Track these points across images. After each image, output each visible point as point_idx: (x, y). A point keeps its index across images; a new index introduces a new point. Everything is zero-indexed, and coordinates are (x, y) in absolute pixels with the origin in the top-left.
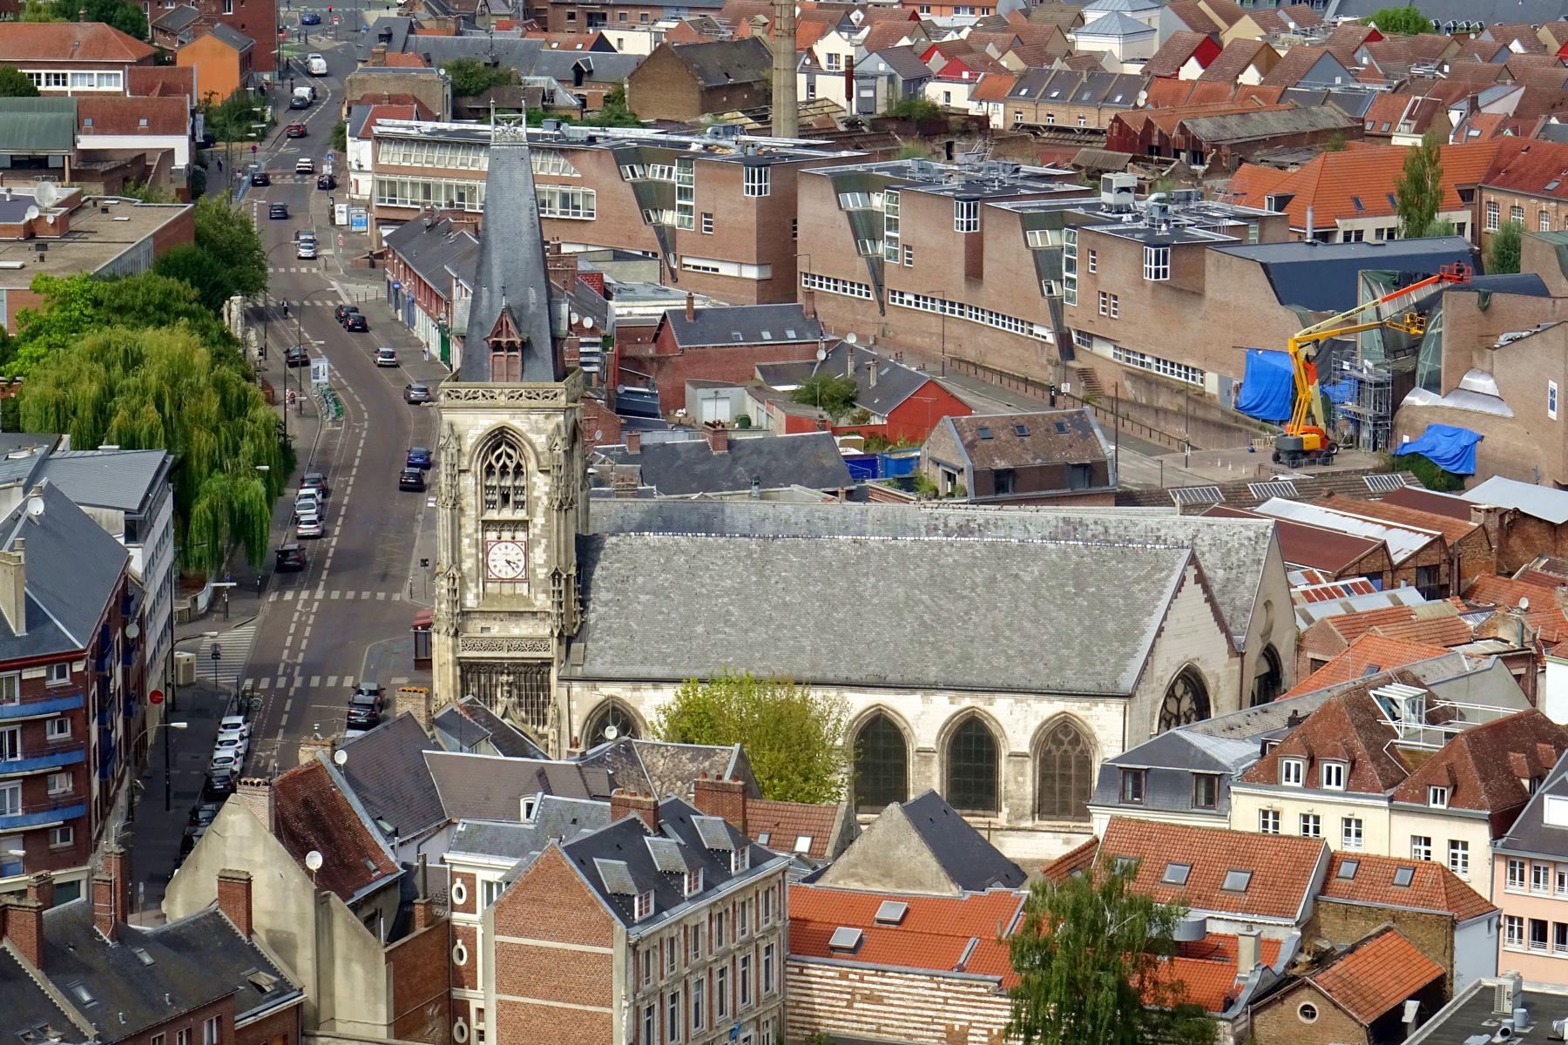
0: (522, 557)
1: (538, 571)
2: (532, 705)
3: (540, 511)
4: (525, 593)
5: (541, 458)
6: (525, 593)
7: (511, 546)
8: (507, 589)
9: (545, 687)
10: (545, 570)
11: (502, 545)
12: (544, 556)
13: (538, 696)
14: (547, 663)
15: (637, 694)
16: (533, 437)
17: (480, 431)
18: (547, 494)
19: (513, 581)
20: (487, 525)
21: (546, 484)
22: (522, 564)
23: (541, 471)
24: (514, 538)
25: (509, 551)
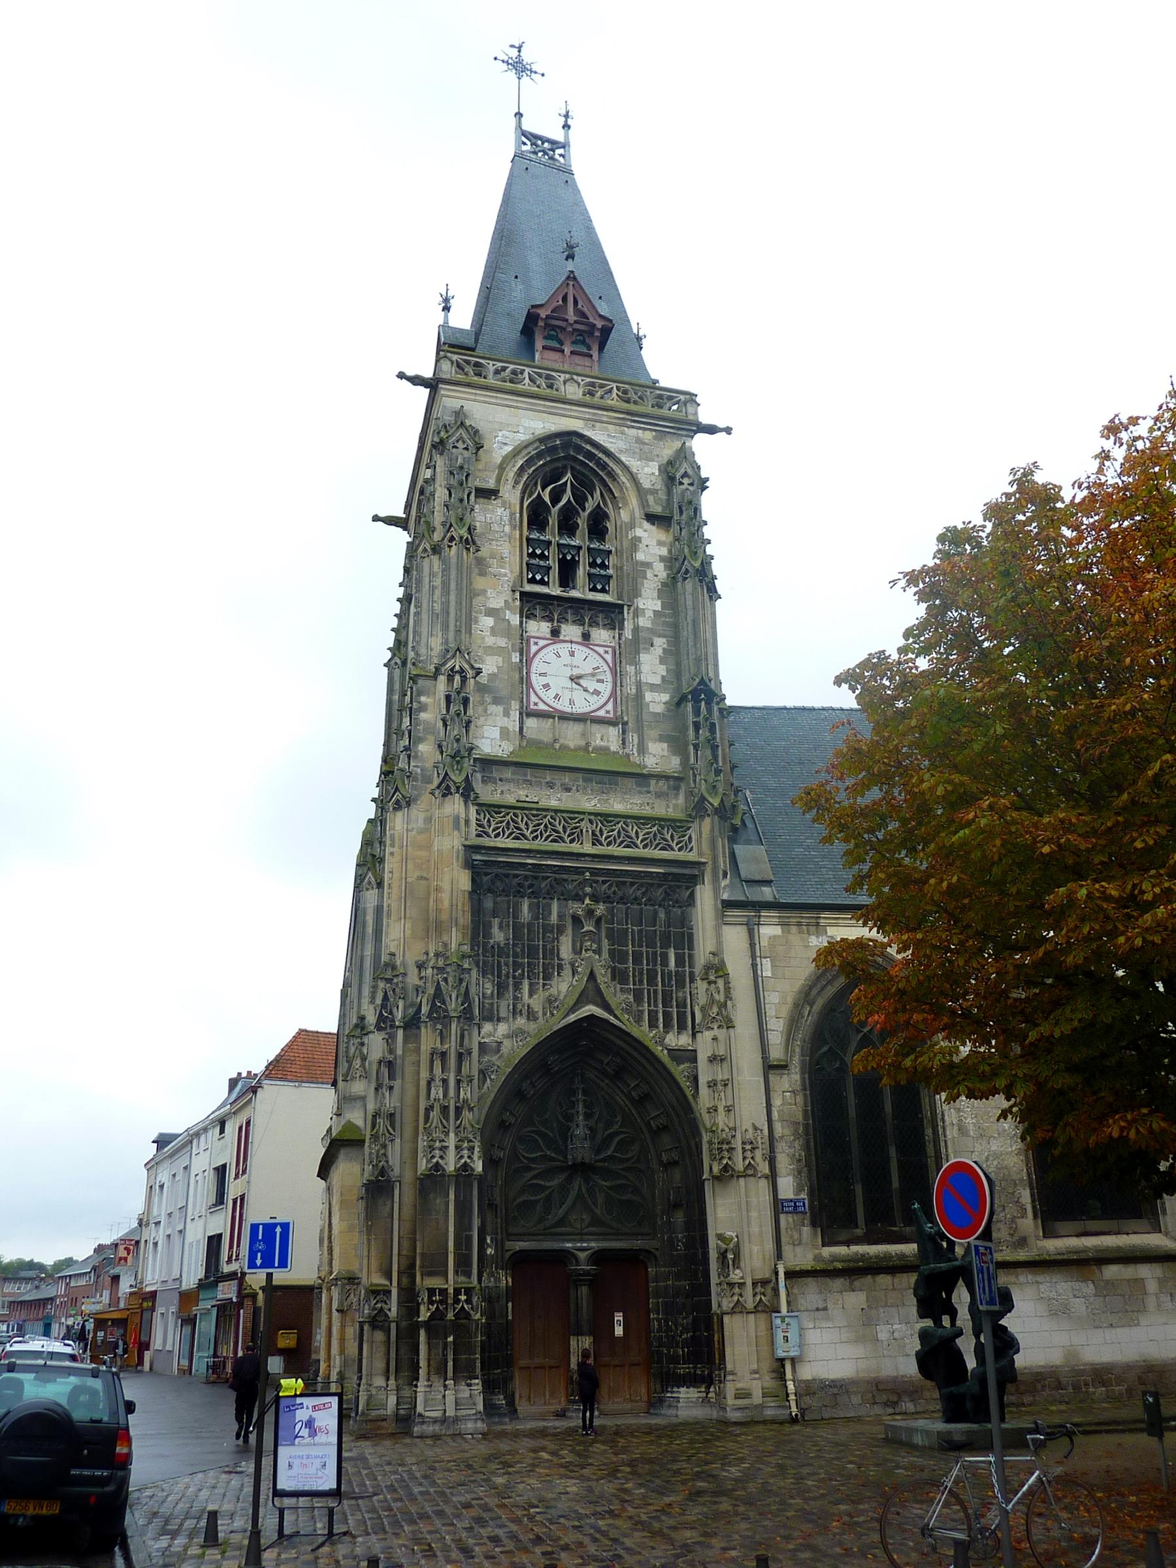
1: (649, 696)
2: (652, 980)
4: (614, 746)
6: (614, 746)
7: (581, 651)
8: (571, 735)
11: (563, 649)
13: (665, 957)
20: (532, 604)
24: (586, 636)
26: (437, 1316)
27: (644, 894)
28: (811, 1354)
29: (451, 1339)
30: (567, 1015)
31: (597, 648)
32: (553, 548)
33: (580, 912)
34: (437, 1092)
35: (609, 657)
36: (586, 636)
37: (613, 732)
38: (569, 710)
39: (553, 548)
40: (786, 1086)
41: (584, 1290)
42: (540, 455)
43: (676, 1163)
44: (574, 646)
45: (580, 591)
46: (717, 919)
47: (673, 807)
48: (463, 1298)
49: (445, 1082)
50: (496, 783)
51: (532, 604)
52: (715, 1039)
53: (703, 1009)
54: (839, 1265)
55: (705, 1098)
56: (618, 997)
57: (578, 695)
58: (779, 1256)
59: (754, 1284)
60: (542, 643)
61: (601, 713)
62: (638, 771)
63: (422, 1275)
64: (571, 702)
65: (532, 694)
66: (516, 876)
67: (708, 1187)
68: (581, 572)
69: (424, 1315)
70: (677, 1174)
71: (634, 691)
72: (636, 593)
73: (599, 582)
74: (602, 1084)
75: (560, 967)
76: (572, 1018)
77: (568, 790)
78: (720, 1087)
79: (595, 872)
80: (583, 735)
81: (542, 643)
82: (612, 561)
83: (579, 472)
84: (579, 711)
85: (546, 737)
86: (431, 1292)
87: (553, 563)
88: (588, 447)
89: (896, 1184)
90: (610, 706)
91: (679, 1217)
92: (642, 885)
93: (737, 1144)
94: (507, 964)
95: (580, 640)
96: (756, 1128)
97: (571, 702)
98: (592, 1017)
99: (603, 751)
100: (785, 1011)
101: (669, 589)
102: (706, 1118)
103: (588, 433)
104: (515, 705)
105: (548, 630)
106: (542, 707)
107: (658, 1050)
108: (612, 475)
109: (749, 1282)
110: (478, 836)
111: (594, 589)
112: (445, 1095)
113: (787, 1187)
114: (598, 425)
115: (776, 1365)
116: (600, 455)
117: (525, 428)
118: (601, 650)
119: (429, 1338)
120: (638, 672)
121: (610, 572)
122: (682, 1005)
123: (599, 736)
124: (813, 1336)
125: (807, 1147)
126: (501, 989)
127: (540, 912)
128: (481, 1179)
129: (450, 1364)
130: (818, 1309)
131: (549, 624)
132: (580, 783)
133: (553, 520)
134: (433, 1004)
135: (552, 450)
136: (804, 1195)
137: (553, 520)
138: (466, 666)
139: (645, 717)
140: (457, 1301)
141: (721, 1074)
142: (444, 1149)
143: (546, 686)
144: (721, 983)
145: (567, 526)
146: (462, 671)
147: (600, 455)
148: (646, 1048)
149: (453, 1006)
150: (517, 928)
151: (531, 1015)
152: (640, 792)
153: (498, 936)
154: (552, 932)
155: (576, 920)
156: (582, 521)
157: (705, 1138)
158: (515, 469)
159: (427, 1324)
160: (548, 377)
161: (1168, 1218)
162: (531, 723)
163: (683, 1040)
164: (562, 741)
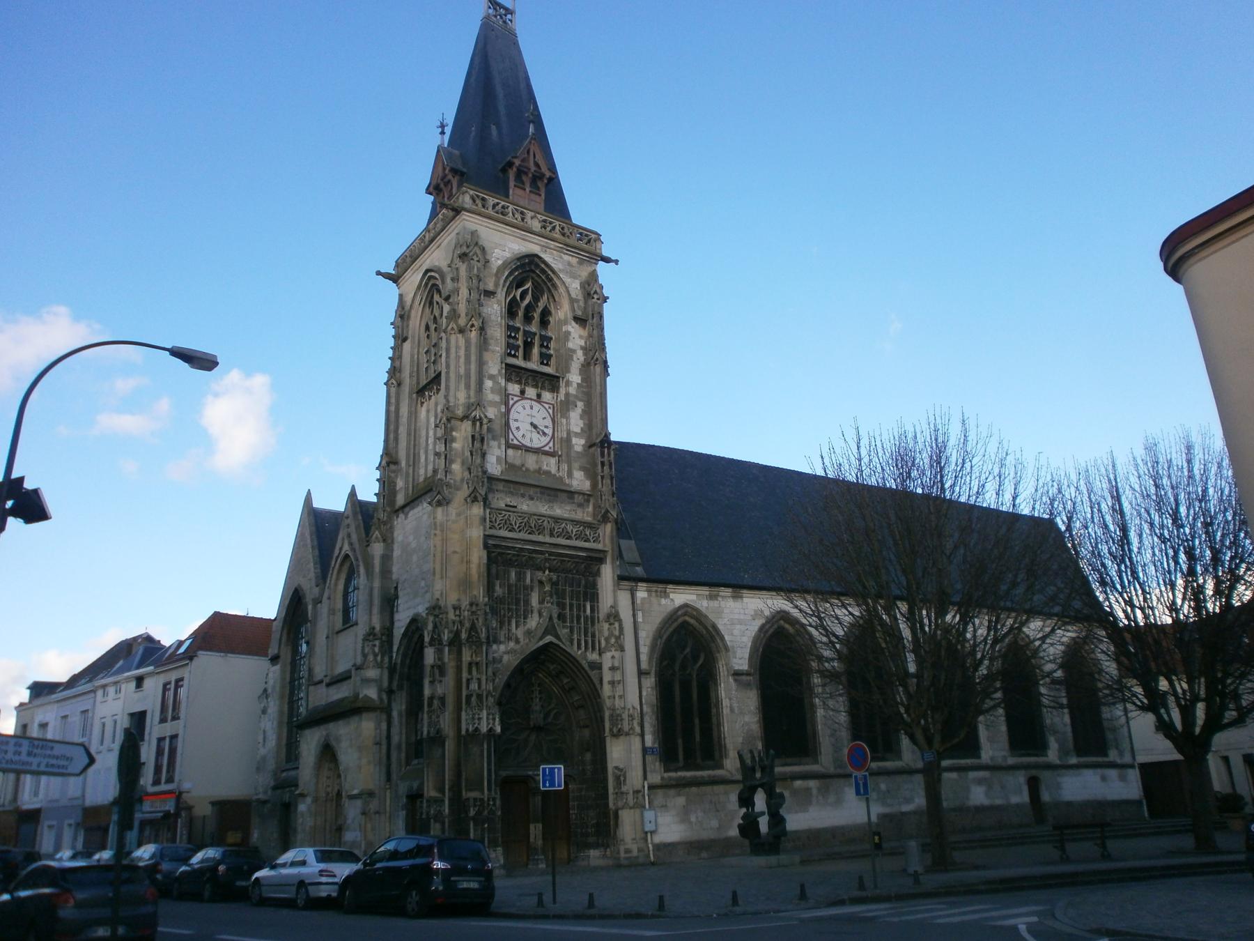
0: (549, 422)
1: (574, 440)
3: (575, 366)
4: (553, 470)
5: (576, 305)
7: (536, 406)
8: (531, 462)
9: (591, 594)
10: (583, 442)
11: (527, 403)
12: (581, 423)
13: (585, 606)
14: (596, 559)
15: (714, 604)
16: (567, 280)
17: (507, 255)
18: (582, 348)
19: (537, 451)
20: (513, 373)
21: (581, 337)
22: (549, 431)
23: (576, 319)
24: (539, 396)
25: (534, 412)
26: (479, 813)
27: (574, 568)
28: (661, 830)
29: (486, 826)
30: (538, 642)
31: (545, 405)
32: (521, 333)
33: (544, 579)
34: (474, 686)
35: (551, 411)
36: (539, 396)
37: (553, 461)
38: (529, 445)
39: (521, 333)
40: (649, 685)
41: (540, 798)
42: (516, 269)
43: (587, 727)
44: (533, 403)
45: (533, 365)
46: (614, 586)
47: (586, 514)
48: (491, 803)
49: (479, 680)
50: (494, 493)
51: (513, 373)
52: (613, 657)
53: (607, 640)
54: (674, 783)
55: (606, 690)
56: (564, 632)
57: (535, 436)
58: (645, 778)
59: (634, 792)
60: (516, 399)
61: (547, 448)
62: (568, 489)
63: (466, 791)
64: (531, 440)
65: (511, 434)
66: (509, 554)
67: (608, 740)
68: (536, 351)
69: (472, 813)
70: (587, 732)
71: (565, 436)
72: (568, 371)
73: (545, 358)
74: (547, 681)
75: (532, 612)
76: (541, 643)
77: (532, 499)
78: (616, 684)
79: (551, 554)
80: (537, 462)
81: (516, 399)
82: (552, 345)
83: (538, 283)
84: (536, 446)
85: (518, 462)
86: (475, 799)
87: (520, 343)
88: (543, 266)
89: (698, 738)
90: (551, 444)
91: (588, 756)
92: (574, 562)
93: (625, 716)
94: (503, 609)
95: (535, 398)
96: (634, 708)
97: (531, 440)
98: (551, 643)
99: (548, 473)
100: (648, 642)
101: (586, 368)
102: (608, 703)
103: (543, 255)
104: (503, 441)
105: (519, 390)
106: (515, 442)
107: (583, 663)
108: (554, 286)
109: (631, 792)
110: (490, 528)
111: (542, 363)
112: (479, 687)
113: (649, 740)
114: (548, 250)
115: (643, 835)
116: (550, 272)
117: (509, 248)
118: (547, 406)
119: (475, 825)
120: (568, 424)
121: (552, 352)
122: (593, 636)
123: (545, 463)
124: (660, 820)
125: (657, 719)
126: (502, 623)
127: (521, 577)
128: (499, 736)
129: (486, 839)
130: (662, 806)
131: (519, 386)
132: (539, 495)
133: (521, 313)
134: (470, 633)
135: (523, 266)
136: (656, 745)
137: (521, 313)
138: (482, 416)
139: (573, 454)
140: (489, 804)
141: (618, 677)
142: (479, 719)
143: (518, 428)
144: (617, 625)
145: (528, 319)
146: (480, 419)
147: (550, 272)
148: (577, 661)
149: (483, 635)
150: (510, 586)
151: (517, 641)
152: (569, 503)
153: (499, 591)
154: (527, 589)
155: (541, 582)
156: (537, 315)
157: (607, 714)
158: (504, 278)
159: (473, 818)
160: (522, 213)
161: (823, 757)
162: (510, 452)
163: (593, 656)
164: (526, 465)
